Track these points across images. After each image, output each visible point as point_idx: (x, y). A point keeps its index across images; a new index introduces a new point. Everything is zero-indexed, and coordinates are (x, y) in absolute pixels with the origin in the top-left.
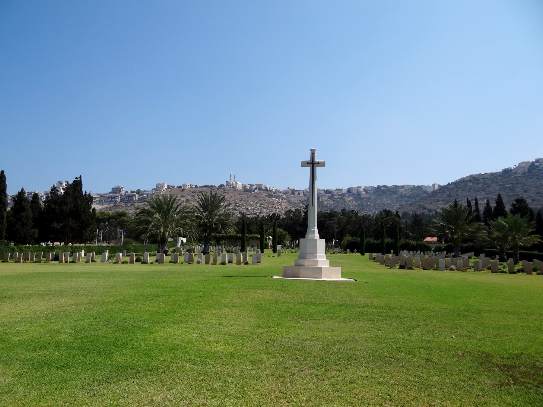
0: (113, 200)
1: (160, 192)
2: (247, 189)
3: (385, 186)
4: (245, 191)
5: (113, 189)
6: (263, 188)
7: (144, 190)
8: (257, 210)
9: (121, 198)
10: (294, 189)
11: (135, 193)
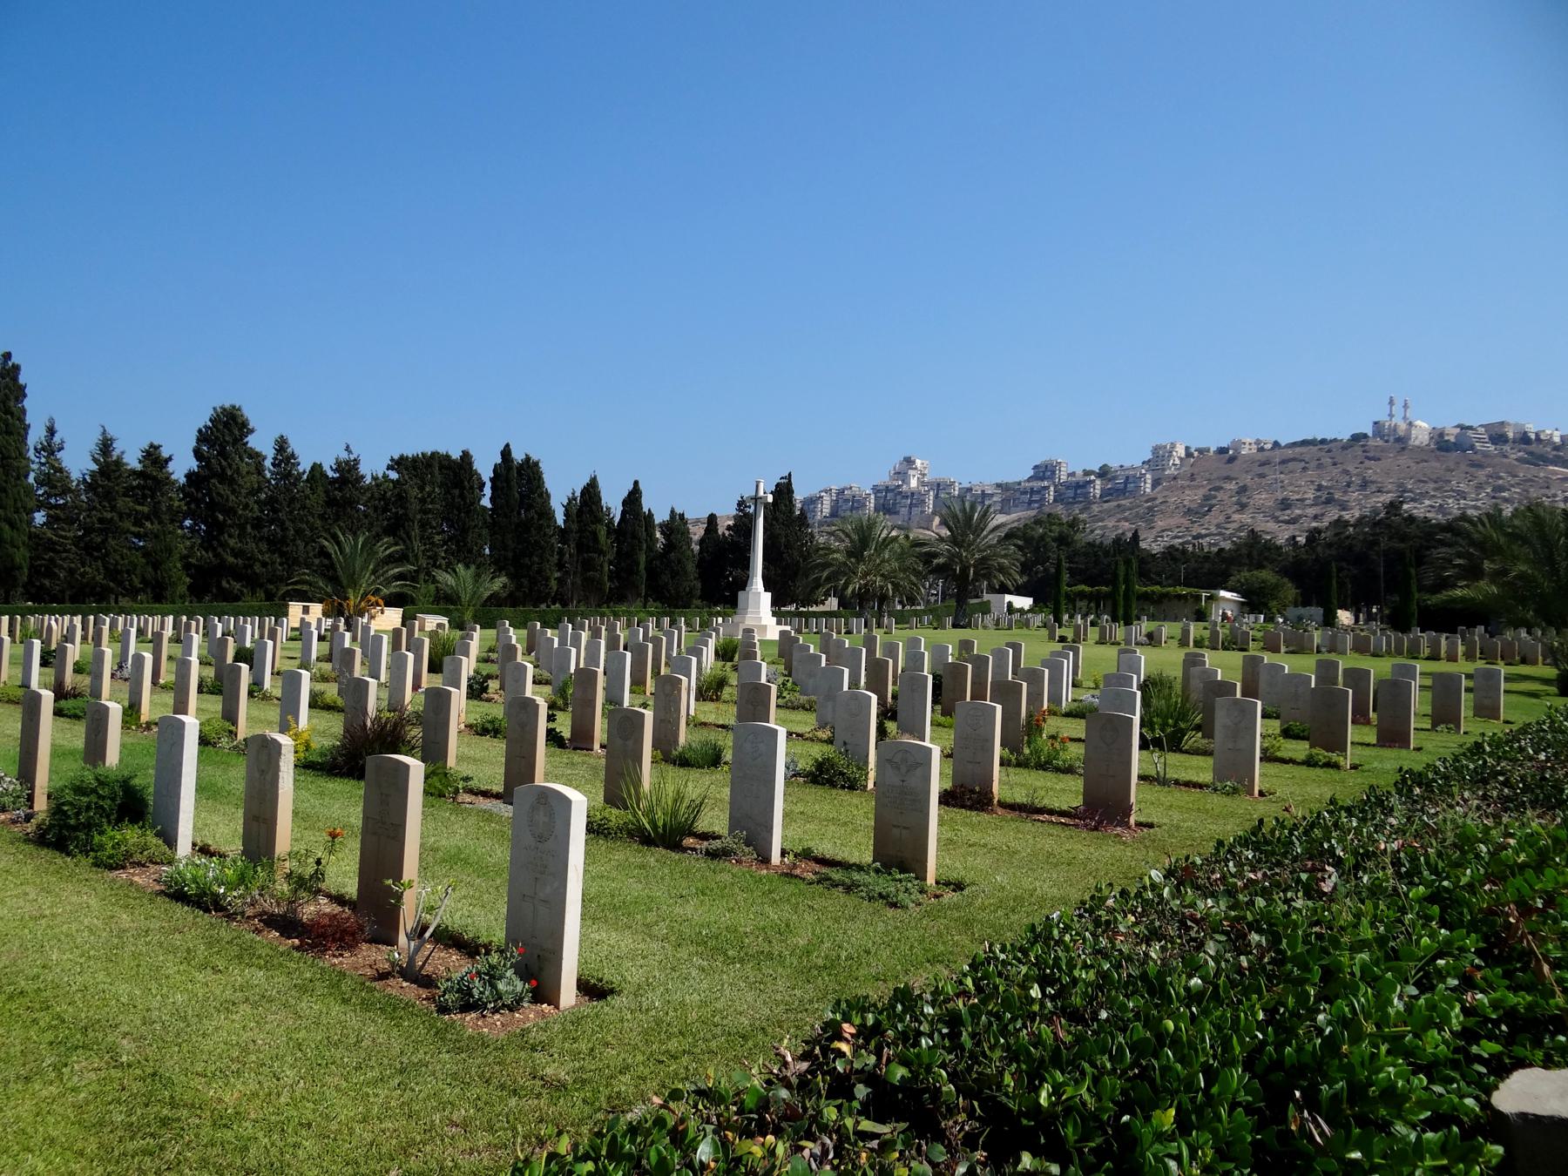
0: (1035, 498)
1: (1164, 470)
2: (1448, 441)
4: (1440, 449)
5: (1036, 467)
6: (1511, 435)
7: (1121, 466)
8: (1476, 508)
9: (1055, 492)
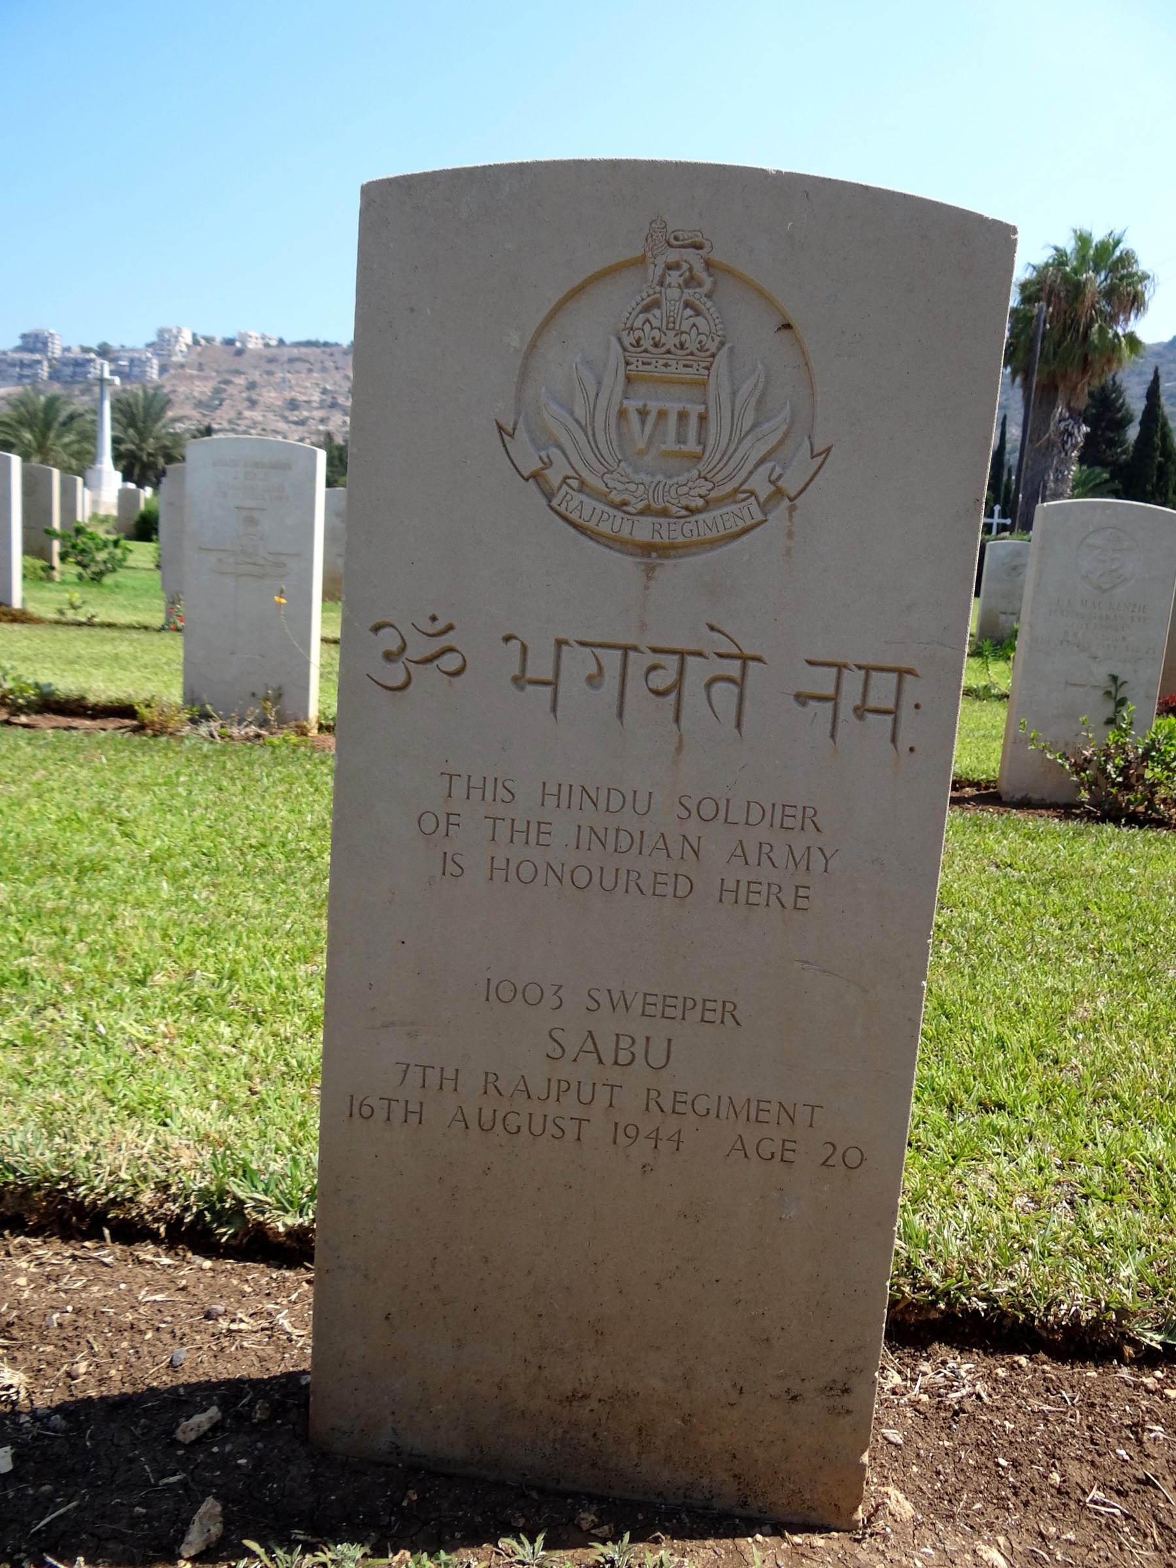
0: (27, 372)
1: (170, 356)
5: (24, 336)
9: (50, 367)
11: (92, 356)
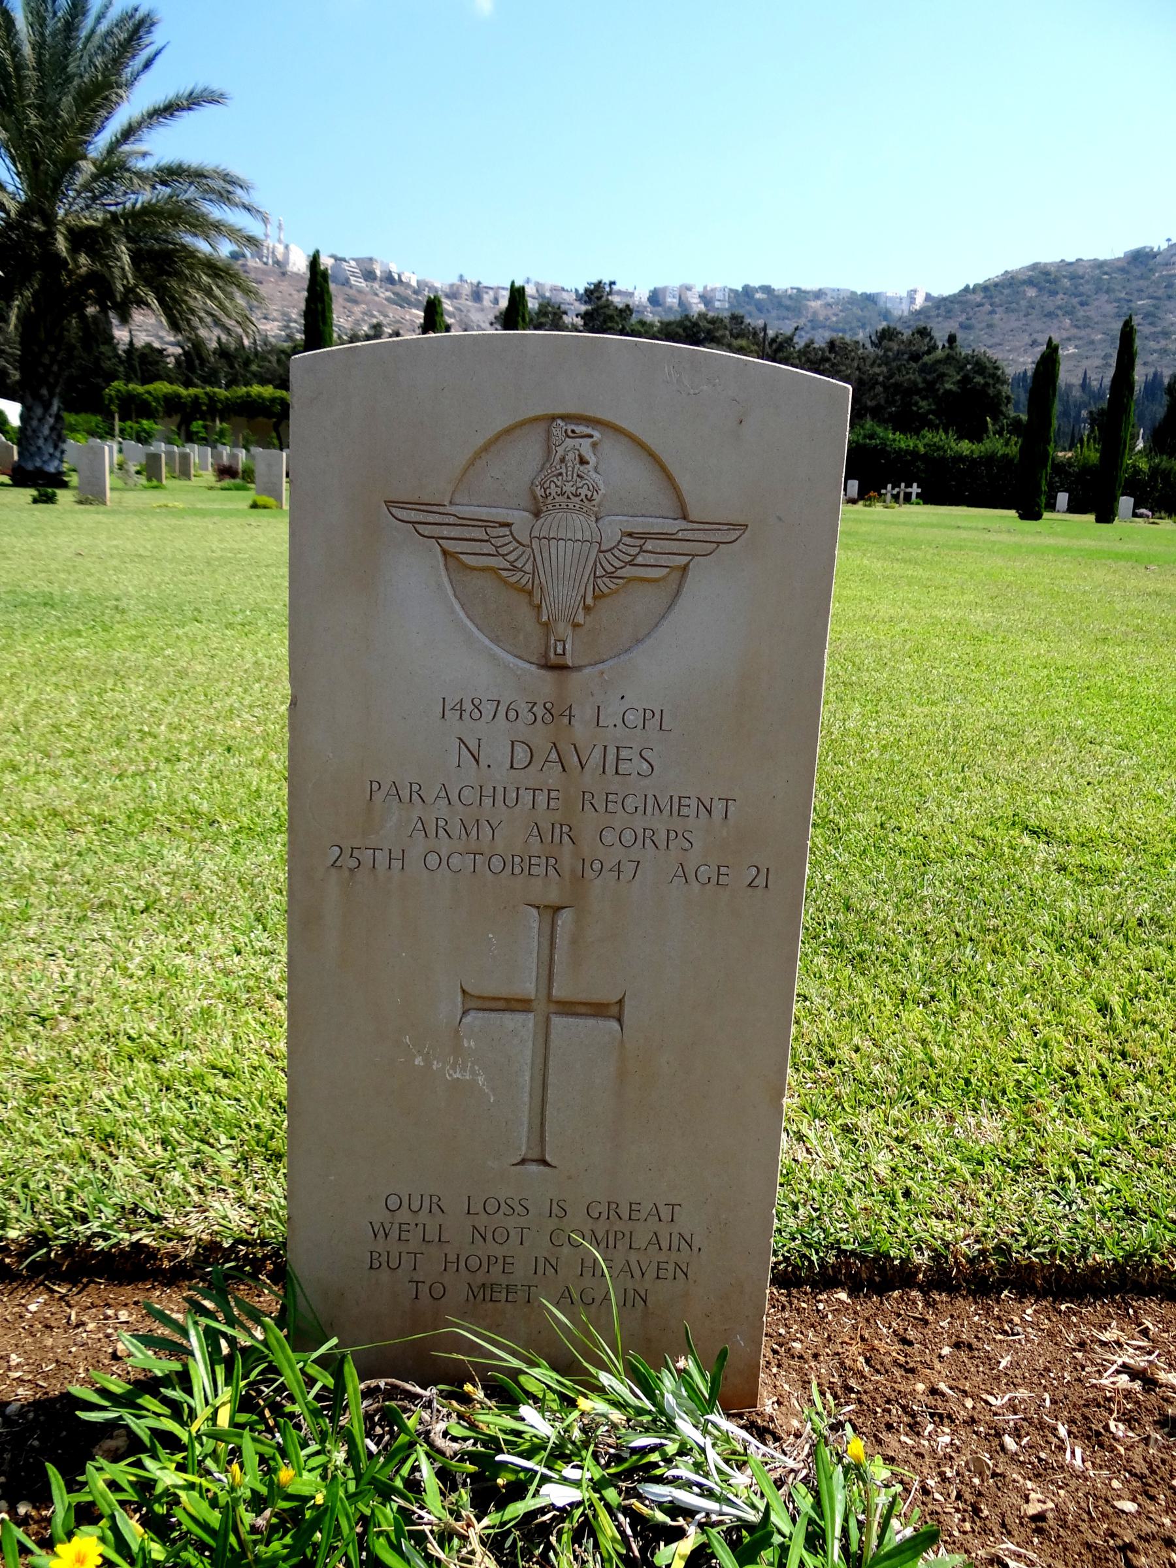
3: (767, 289)
6: (378, 273)
10: (479, 283)
